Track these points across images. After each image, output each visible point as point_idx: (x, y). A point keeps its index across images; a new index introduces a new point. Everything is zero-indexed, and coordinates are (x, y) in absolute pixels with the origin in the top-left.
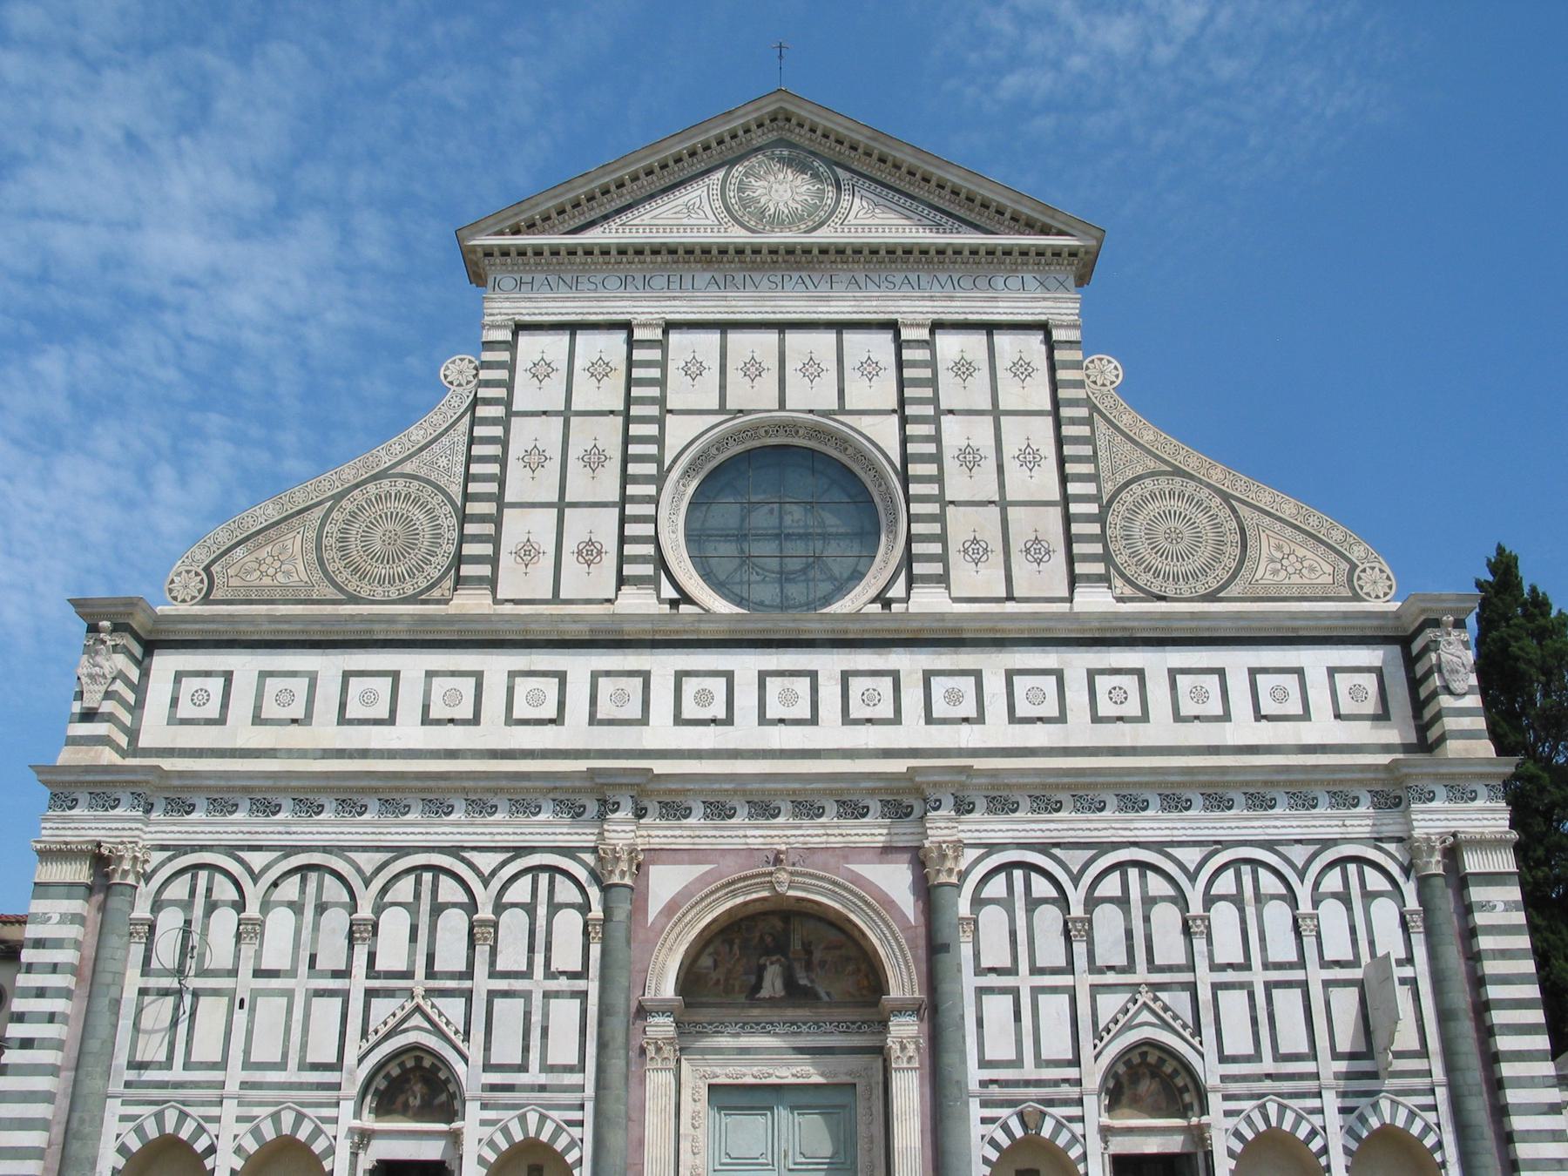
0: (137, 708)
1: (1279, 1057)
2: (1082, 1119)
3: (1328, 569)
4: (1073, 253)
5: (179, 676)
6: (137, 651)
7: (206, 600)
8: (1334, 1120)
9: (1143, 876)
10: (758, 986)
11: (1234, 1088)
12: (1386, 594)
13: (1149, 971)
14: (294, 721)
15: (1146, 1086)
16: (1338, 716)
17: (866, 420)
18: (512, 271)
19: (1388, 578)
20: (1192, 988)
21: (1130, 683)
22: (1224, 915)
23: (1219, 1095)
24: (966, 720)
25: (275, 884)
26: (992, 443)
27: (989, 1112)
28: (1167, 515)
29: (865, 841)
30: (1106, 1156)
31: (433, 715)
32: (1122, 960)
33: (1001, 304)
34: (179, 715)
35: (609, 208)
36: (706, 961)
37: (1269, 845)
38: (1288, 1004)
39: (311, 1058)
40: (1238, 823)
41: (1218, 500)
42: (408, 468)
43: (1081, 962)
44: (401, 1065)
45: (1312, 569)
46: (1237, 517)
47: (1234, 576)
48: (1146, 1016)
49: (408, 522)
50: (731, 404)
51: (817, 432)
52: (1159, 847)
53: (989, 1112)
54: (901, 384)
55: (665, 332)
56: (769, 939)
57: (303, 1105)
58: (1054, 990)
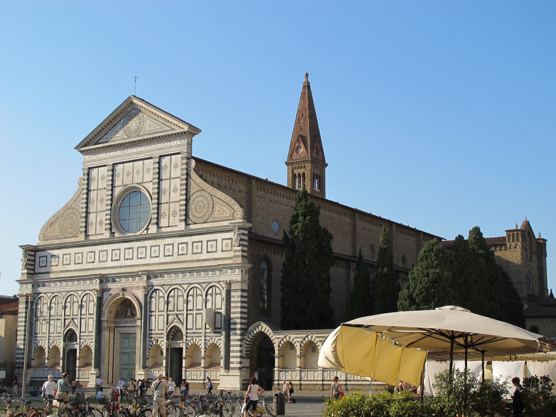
0: (34, 265)
1: (196, 329)
2: (163, 341)
3: (229, 212)
4: (185, 132)
5: (40, 257)
6: (33, 253)
7: (45, 240)
8: (203, 341)
9: (178, 291)
10: (127, 314)
11: (188, 335)
12: (240, 218)
13: (177, 311)
14: (56, 265)
15: (179, 334)
16: (222, 251)
17: (147, 184)
18: (87, 155)
19: (241, 213)
20: (183, 314)
21: (185, 246)
22: (190, 298)
23: (185, 336)
24: (156, 257)
25: (52, 299)
26: (169, 187)
27: (150, 340)
28: (198, 202)
29: (135, 285)
30: (169, 348)
31: (76, 262)
32: (172, 309)
33: (172, 149)
34: (41, 265)
35: (103, 135)
36: (119, 309)
37: (199, 284)
38: (199, 317)
39: (58, 331)
40: (195, 278)
41: (210, 196)
42: (73, 206)
43: (166, 310)
44: (71, 332)
45: (226, 213)
46: (213, 200)
47: (210, 216)
48: (175, 320)
49: (72, 218)
50: (124, 184)
51: (139, 188)
52: (180, 285)
53: (150, 340)
54: (154, 174)
55: (113, 167)
56: (128, 304)
57: (57, 340)
58: (161, 315)
